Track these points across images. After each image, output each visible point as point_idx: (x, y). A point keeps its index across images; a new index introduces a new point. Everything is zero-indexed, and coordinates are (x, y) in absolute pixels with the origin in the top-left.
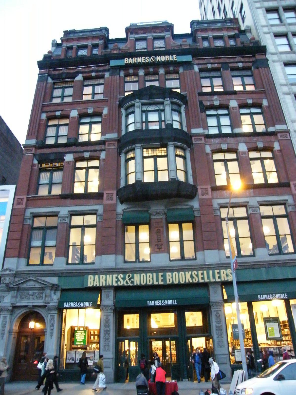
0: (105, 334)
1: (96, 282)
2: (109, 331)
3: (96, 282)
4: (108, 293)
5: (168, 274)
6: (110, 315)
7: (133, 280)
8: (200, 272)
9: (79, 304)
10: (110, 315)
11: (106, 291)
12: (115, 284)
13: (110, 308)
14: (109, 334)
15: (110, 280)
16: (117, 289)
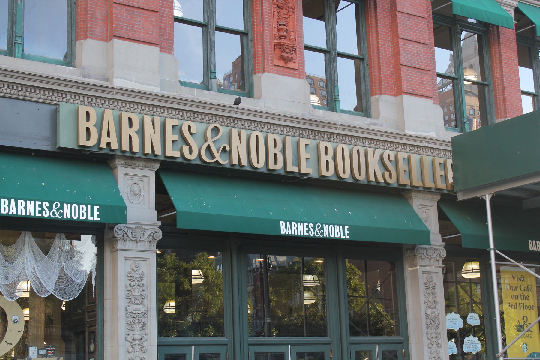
0: (130, 326)
1: (109, 136)
2: (144, 314)
3: (109, 136)
4: (136, 180)
5: (323, 144)
6: (145, 259)
7: (228, 149)
8: (402, 155)
9: (54, 209)
10: (145, 259)
11: (130, 171)
12: (171, 152)
13: (146, 235)
14: (143, 327)
15: (156, 136)
16: (170, 169)
